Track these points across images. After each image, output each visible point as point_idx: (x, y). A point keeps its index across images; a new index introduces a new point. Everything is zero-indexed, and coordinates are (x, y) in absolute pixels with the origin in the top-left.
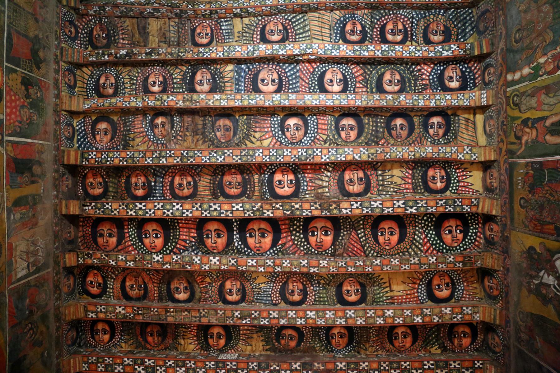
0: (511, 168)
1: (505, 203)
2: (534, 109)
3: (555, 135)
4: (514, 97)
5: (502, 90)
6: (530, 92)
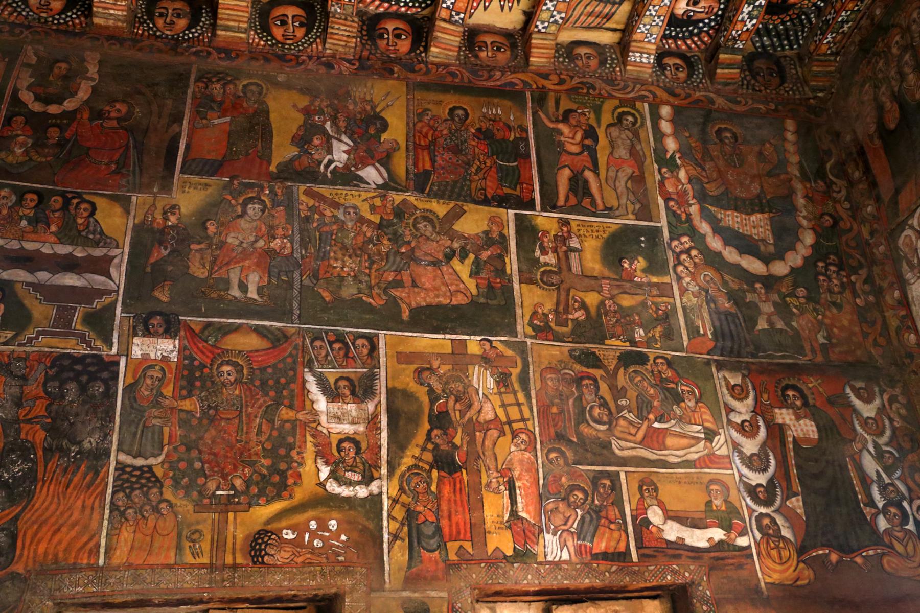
0: (513, 95)
1: (453, 74)
2: (611, 153)
3: (571, 185)
4: (633, 115)
5: (646, 93)
6: (638, 147)
